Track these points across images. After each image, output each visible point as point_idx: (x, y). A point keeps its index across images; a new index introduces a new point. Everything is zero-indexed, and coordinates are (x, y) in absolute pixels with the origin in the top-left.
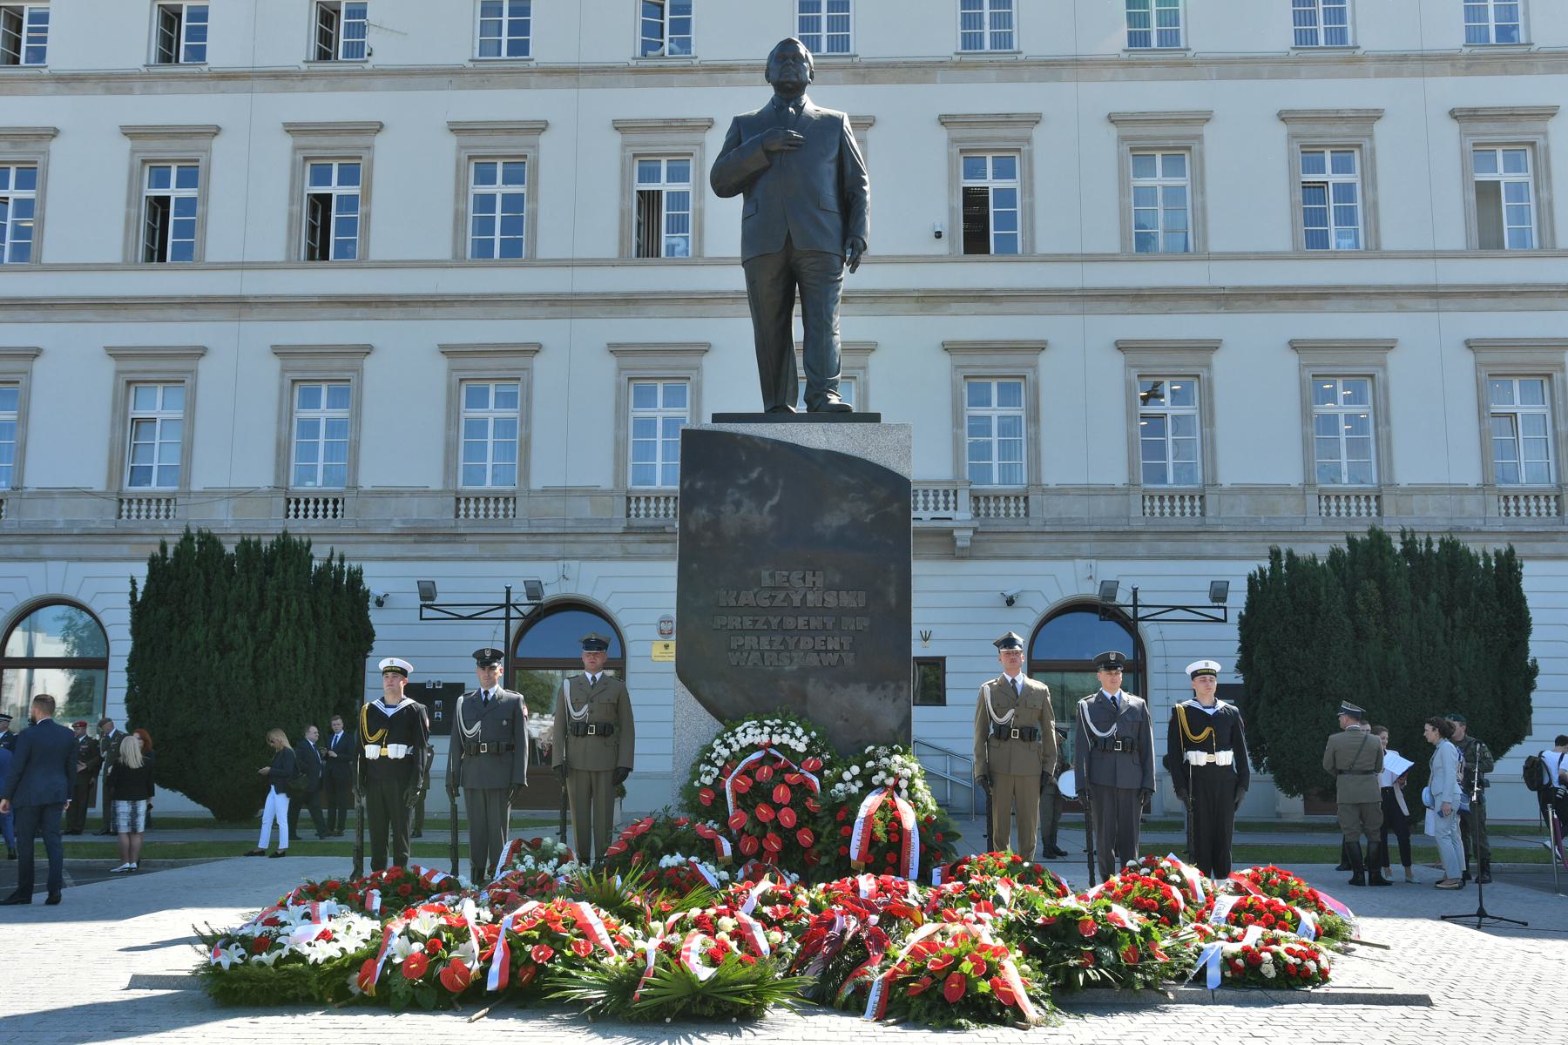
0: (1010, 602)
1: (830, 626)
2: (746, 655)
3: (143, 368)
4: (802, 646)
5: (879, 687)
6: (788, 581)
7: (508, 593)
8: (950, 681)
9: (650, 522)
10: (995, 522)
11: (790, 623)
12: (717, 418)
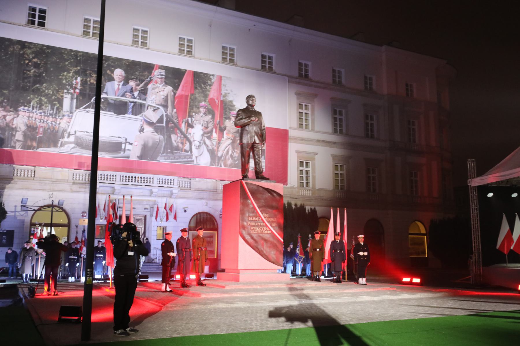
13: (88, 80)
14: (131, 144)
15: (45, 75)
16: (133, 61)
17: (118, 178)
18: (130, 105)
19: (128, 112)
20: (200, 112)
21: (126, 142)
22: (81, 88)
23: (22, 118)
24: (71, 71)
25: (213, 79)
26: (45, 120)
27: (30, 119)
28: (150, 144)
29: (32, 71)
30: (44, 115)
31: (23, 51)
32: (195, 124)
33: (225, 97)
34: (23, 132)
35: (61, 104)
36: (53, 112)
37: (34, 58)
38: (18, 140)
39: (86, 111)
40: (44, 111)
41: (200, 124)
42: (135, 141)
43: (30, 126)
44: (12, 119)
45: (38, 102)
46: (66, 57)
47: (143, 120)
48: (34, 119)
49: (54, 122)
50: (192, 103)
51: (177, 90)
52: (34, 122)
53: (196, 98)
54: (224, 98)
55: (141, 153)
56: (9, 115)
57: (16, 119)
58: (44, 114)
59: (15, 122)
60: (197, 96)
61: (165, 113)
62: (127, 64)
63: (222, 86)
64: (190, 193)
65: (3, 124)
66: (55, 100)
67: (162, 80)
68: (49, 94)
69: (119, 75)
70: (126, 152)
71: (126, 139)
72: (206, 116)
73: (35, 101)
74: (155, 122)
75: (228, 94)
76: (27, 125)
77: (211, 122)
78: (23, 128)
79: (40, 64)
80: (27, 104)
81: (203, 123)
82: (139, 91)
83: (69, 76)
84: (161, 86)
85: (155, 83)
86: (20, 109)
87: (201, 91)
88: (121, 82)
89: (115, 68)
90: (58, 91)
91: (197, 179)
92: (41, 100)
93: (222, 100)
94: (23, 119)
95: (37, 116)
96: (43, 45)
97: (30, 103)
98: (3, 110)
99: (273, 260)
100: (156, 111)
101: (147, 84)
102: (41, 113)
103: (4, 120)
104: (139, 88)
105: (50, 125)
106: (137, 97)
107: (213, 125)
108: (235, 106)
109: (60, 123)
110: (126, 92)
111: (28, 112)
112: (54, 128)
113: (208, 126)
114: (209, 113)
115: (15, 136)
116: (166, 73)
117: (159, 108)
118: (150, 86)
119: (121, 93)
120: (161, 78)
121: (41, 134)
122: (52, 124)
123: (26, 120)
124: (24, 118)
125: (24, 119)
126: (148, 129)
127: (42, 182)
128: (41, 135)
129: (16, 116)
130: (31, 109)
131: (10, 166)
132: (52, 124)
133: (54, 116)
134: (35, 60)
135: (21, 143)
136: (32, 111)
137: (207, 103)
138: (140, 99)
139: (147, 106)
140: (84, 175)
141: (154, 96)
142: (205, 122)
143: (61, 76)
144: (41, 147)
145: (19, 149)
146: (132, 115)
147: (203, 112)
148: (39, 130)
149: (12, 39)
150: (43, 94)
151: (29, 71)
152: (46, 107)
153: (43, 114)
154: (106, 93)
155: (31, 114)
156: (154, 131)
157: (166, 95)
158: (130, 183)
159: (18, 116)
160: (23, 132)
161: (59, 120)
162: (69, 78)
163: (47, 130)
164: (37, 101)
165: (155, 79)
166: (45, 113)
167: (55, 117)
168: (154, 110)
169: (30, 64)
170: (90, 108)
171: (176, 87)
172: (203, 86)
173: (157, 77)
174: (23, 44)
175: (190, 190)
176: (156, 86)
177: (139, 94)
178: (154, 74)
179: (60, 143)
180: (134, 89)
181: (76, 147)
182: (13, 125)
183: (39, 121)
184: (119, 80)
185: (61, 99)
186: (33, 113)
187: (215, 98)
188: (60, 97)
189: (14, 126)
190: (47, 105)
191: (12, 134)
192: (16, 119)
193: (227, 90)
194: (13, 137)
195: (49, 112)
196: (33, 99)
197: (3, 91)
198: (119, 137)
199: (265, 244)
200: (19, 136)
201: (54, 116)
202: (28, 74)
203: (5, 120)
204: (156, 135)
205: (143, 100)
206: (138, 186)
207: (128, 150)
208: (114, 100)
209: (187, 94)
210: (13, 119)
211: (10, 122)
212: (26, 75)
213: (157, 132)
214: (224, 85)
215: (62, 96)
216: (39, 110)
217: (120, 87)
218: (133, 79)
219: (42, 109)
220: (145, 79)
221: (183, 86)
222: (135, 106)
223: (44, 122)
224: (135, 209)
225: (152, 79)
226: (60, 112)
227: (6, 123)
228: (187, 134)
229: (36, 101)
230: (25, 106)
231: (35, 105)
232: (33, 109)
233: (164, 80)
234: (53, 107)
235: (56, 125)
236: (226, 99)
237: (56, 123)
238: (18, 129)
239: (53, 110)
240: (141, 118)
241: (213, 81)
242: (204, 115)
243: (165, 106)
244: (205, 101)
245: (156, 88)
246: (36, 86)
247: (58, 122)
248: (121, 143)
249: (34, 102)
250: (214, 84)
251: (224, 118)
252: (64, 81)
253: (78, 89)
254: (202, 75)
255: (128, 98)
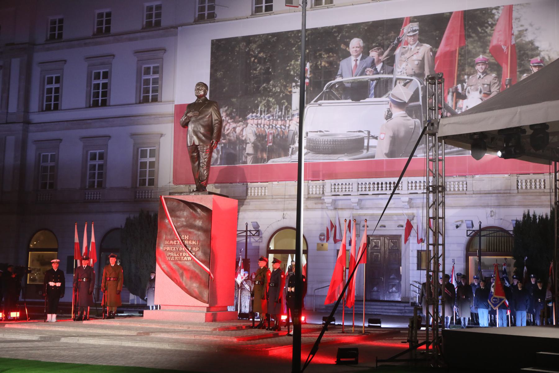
0: (457, 227)
7: (247, 226)
13: (319, 63)
14: (376, 138)
15: (272, 70)
16: (373, 22)
17: (355, 187)
18: (372, 84)
19: (370, 94)
20: (476, 72)
21: (370, 136)
22: (310, 76)
23: (251, 127)
24: (299, 57)
25: (496, 13)
26: (274, 125)
27: (259, 126)
28: (402, 134)
29: (258, 69)
30: (272, 119)
31: (248, 47)
32: (469, 92)
33: (520, 37)
34: (253, 143)
35: (290, 103)
36: (282, 114)
37: (259, 53)
38: (248, 154)
39: (317, 105)
40: (272, 114)
41: (477, 90)
42: (381, 133)
43: (259, 134)
44: (241, 130)
45: (266, 104)
46: (292, 42)
47: (390, 102)
48: (262, 126)
49: (283, 125)
50: (462, 61)
51: (437, 47)
52: (262, 129)
53: (469, 52)
54: (518, 40)
55: (390, 148)
56: (238, 126)
57: (245, 130)
58: (273, 118)
59: (244, 134)
60: (470, 47)
61: (421, 84)
62: (366, 28)
63: (513, 21)
64: (466, 199)
65: (234, 137)
66: (283, 98)
67: (415, 37)
68: (277, 92)
69: (356, 47)
70: (370, 149)
71: (369, 132)
72: (488, 76)
73: (263, 104)
74: (407, 102)
75: (525, 32)
76: (256, 134)
77: (495, 83)
78: (252, 138)
79: (265, 58)
80: (255, 109)
81: (482, 88)
82: (383, 62)
83: (297, 64)
84: (413, 47)
85: (404, 45)
86: (248, 116)
87: (476, 38)
88: (358, 55)
89: (351, 39)
90: (285, 86)
91: (477, 176)
92: (268, 101)
93: (514, 44)
94: (252, 128)
95: (266, 121)
96: (268, 34)
97: (258, 107)
98: (232, 122)
99: (195, 295)
100: (407, 85)
101: (394, 49)
102: (269, 117)
103: (234, 132)
104: (382, 58)
105: (280, 129)
106: (381, 70)
107: (498, 88)
108: (539, 49)
109: (290, 125)
110: (365, 68)
111: (256, 119)
112: (283, 133)
113: (490, 91)
114: (492, 70)
115: (245, 149)
116: (420, 26)
117: (411, 80)
118: (398, 52)
119: (360, 70)
120: (414, 36)
121: (270, 143)
122: (281, 128)
123: (254, 129)
124: (253, 127)
125: (253, 128)
126: (398, 113)
127: (273, 200)
128: (271, 144)
129: (245, 126)
130: (259, 115)
131: (243, 185)
132: (281, 128)
133: (283, 118)
134: (261, 55)
135: (252, 156)
136: (260, 117)
137: (487, 55)
138: (385, 74)
139: (394, 80)
140: (322, 187)
141: (404, 65)
142: (486, 86)
143: (288, 66)
144: (272, 158)
145: (250, 164)
146: (375, 97)
147: (481, 71)
148: (268, 137)
149: (237, 38)
150: (270, 94)
151: (255, 70)
152: (274, 109)
153: (271, 118)
154: (341, 76)
155: (259, 120)
156: (406, 115)
157: (421, 59)
158: (371, 192)
159: (247, 126)
160: (252, 144)
161: (288, 121)
162: (297, 67)
163: (277, 137)
164: (265, 103)
165: (404, 39)
166: (274, 117)
167: (284, 120)
168: (405, 85)
169: (256, 61)
170: (322, 100)
171: (435, 44)
172: (480, 30)
173: (408, 36)
174: (248, 40)
175: (466, 194)
176: (406, 49)
177: (383, 66)
178: (403, 32)
179: (290, 150)
180: (376, 60)
181: (309, 153)
182: (242, 137)
183: (268, 127)
184: (356, 54)
185: (289, 95)
186: (262, 119)
187: (502, 43)
188: (288, 93)
189: (244, 138)
190: (275, 106)
191: (242, 147)
192: (245, 130)
193: (522, 26)
194: (244, 151)
195: (277, 115)
196: (261, 102)
197: (231, 100)
198: (360, 131)
199: (185, 274)
200: (249, 149)
201: (283, 118)
202: (255, 74)
203: (236, 132)
204: (409, 120)
205: (389, 74)
206: (380, 196)
207: (372, 147)
208: (351, 82)
209: (453, 49)
210: (242, 130)
211: (240, 134)
212: (252, 75)
213: (410, 115)
214: (516, 19)
215: (291, 92)
216: (267, 114)
217: (358, 62)
218: (376, 46)
219: (271, 112)
220: (391, 42)
221: (448, 39)
222: (378, 84)
223: (272, 128)
224: (385, 227)
225: (400, 39)
226: (288, 111)
227: (236, 136)
228: (456, 110)
229: (263, 104)
230: (253, 113)
231: (263, 110)
232: (261, 114)
233: (417, 37)
234: (282, 107)
235: (285, 129)
236: (522, 40)
237: (285, 126)
238: (248, 141)
239: (282, 111)
240: (388, 99)
241: (496, 17)
242: (483, 74)
243: (420, 75)
244: (484, 53)
245: (406, 52)
246: (263, 86)
247: (287, 125)
248: (361, 140)
249: (262, 106)
250: (498, 23)
251: (518, 73)
252: (292, 73)
253: (308, 78)
254: (478, 12)
255: (369, 75)
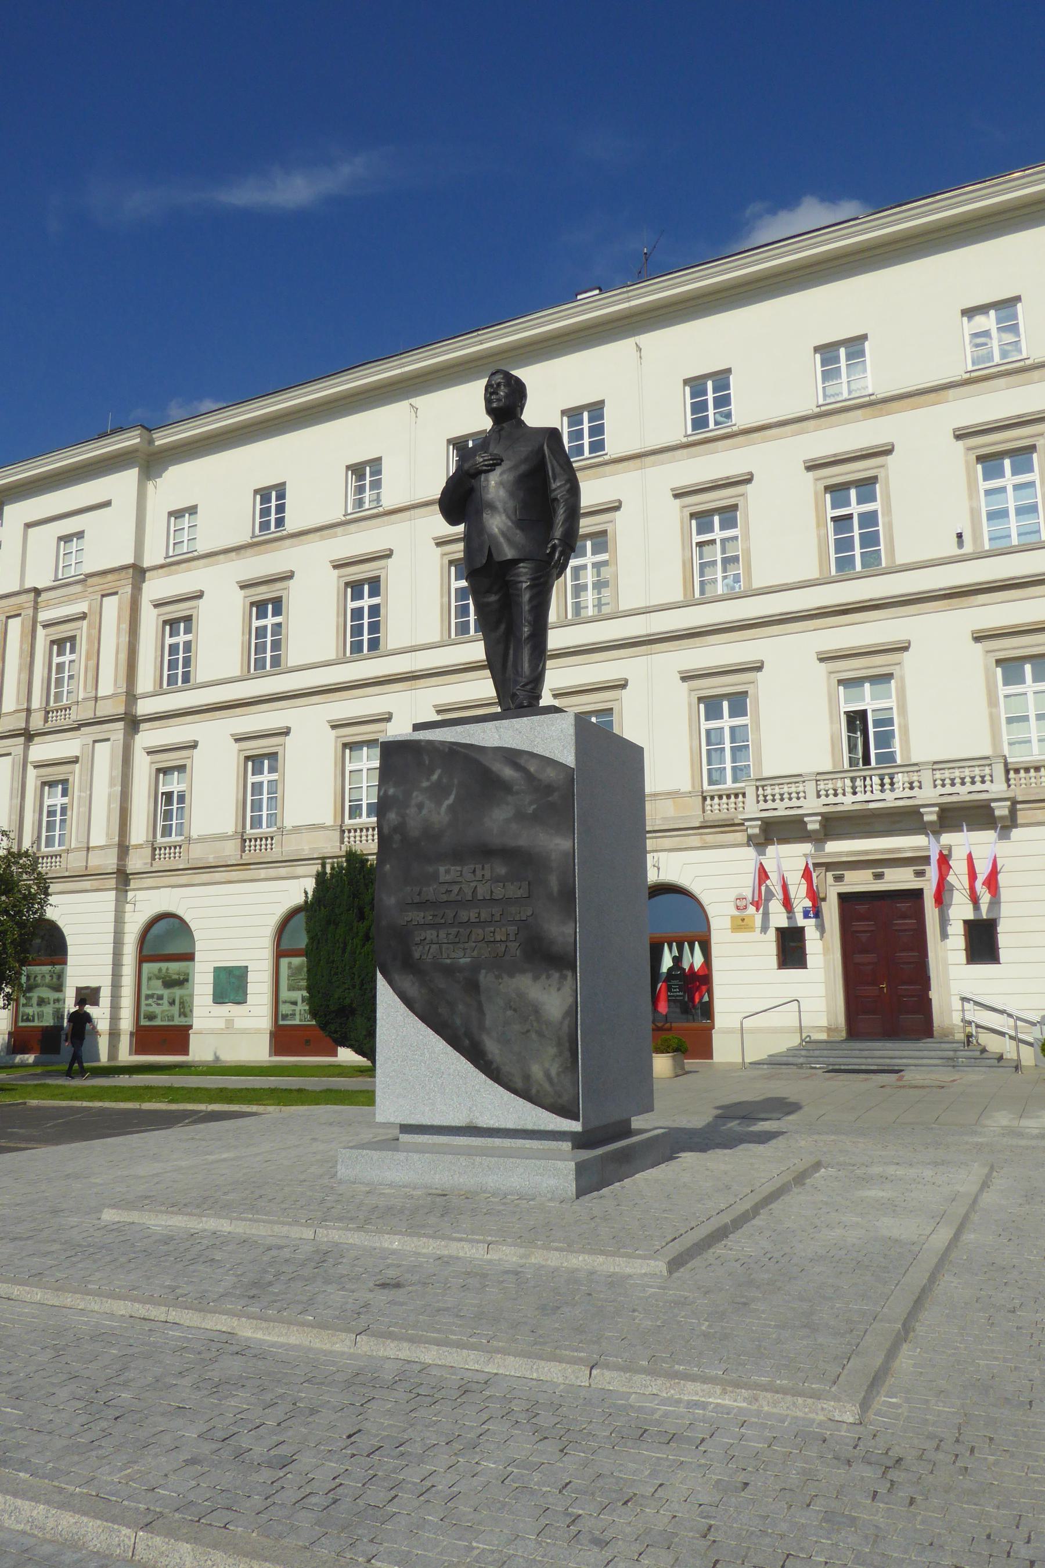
1: (497, 918)
2: (427, 948)
3: (352, 733)
4: (473, 937)
5: (544, 977)
6: (461, 875)
8: (1003, 940)
9: (724, 815)
10: (1037, 790)
11: (464, 916)
12: (417, 727)
